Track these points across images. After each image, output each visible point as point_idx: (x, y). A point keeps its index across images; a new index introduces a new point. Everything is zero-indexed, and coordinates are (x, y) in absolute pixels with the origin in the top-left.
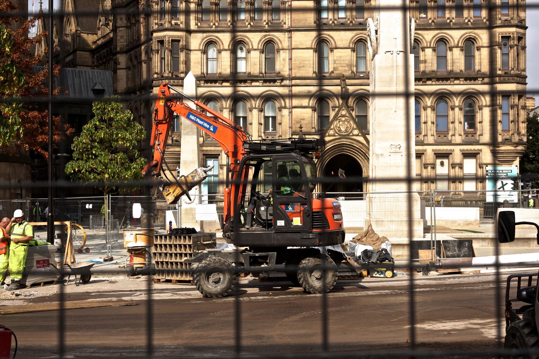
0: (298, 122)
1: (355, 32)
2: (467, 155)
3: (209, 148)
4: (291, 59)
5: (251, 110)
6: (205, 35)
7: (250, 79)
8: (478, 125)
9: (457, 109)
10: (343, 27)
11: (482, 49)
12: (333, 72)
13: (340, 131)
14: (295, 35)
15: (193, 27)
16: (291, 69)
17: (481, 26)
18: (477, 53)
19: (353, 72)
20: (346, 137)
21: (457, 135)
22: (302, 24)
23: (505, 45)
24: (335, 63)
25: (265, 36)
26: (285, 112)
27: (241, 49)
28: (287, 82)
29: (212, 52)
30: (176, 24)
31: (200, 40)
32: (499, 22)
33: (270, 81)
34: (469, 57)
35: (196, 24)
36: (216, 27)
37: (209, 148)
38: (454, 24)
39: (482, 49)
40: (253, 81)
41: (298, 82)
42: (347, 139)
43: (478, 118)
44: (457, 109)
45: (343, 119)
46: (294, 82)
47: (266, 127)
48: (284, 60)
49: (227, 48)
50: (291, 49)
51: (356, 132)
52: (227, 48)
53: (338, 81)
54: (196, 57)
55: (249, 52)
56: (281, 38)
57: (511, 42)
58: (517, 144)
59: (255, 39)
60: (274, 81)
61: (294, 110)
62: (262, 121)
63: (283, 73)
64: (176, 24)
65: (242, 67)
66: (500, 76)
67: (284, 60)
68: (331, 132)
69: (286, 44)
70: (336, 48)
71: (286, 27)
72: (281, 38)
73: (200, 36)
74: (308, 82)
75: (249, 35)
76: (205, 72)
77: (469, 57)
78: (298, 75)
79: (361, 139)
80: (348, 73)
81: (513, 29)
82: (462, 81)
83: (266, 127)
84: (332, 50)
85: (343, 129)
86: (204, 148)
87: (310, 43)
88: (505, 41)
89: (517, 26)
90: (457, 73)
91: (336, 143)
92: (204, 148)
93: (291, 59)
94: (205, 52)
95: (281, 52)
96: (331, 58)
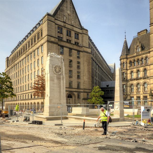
7: (141, 78)
15: (128, 68)
26: (149, 85)
28: (149, 78)
33: (145, 78)
40: (141, 79)
46: (151, 78)
49: (135, 72)
50: (150, 70)
52: (135, 72)
56: (148, 67)
59: (141, 69)
60: (146, 78)
63: (148, 76)
67: (149, 73)
69: (149, 69)
71: (149, 64)
72: (148, 67)
73: (130, 70)
75: (140, 68)
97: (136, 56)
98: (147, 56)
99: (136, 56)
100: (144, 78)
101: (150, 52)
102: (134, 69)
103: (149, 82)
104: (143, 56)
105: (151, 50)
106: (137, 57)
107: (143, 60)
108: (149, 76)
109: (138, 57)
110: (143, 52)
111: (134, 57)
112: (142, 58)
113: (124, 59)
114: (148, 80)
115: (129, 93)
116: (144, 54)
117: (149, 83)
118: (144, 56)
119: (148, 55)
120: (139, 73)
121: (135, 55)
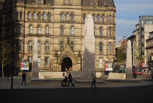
0: (55, 48)
1: (71, 24)
2: (100, 58)
3: (30, 55)
4: (53, 31)
5: (42, 44)
6: (29, 23)
8: (103, 50)
9: (98, 46)
10: (68, 22)
11: (104, 30)
12: (65, 35)
13: (67, 51)
14: (55, 24)
15: (26, 20)
16: (53, 33)
17: (104, 24)
18: (103, 31)
19: (70, 35)
20: (68, 52)
21: (98, 53)
22: (56, 21)
23: (110, 29)
24: (65, 32)
25: (46, 24)
26: (51, 45)
27: (39, 27)
28: (52, 37)
29: (31, 28)
30: (21, 20)
31: (28, 24)
32: (109, 23)
34: (101, 32)
35: (27, 20)
36: (33, 21)
37: (30, 55)
38: (97, 23)
39: (104, 30)
41: (55, 37)
42: (68, 53)
43: (103, 48)
44: (98, 46)
45: (68, 48)
46: (54, 37)
47: (46, 49)
48: (51, 31)
50: (53, 28)
51: (71, 51)
52: (35, 27)
53: (66, 37)
54: (27, 29)
55: (42, 28)
56: (51, 25)
57: (112, 29)
58: (113, 55)
61: (54, 45)
62: (45, 48)
64: (21, 20)
65: (39, 32)
66: (109, 37)
67: (51, 31)
68: (64, 51)
69: (52, 26)
70: (66, 28)
71: (52, 22)
73: (28, 23)
74: (58, 37)
76: (29, 33)
77: (101, 32)
78: (55, 35)
79: (72, 53)
80: (69, 35)
81: (112, 25)
82: (99, 38)
83: (46, 49)
84: (65, 28)
85: (67, 50)
86: (28, 55)
87: (59, 26)
88: (110, 28)
89: (113, 24)
90: (98, 36)
91: (66, 54)
92: (28, 55)
93: (53, 31)
94: (29, 28)
95: (51, 28)
96: (64, 31)
97: (38, 8)
98: (50, 11)
99: (38, 8)
100: (47, 35)
101: (54, 8)
102: (33, 23)
103: (52, 41)
104: (45, 10)
105: (55, 6)
106: (38, 10)
107: (45, 15)
108: (52, 34)
109: (40, 10)
110: (46, 6)
111: (35, 8)
112: (44, 13)
113: (22, 7)
114: (50, 39)
115: (26, 52)
116: (47, 8)
117: (52, 42)
118: (47, 11)
119: (52, 11)
120: (39, 29)
121: (36, 6)
